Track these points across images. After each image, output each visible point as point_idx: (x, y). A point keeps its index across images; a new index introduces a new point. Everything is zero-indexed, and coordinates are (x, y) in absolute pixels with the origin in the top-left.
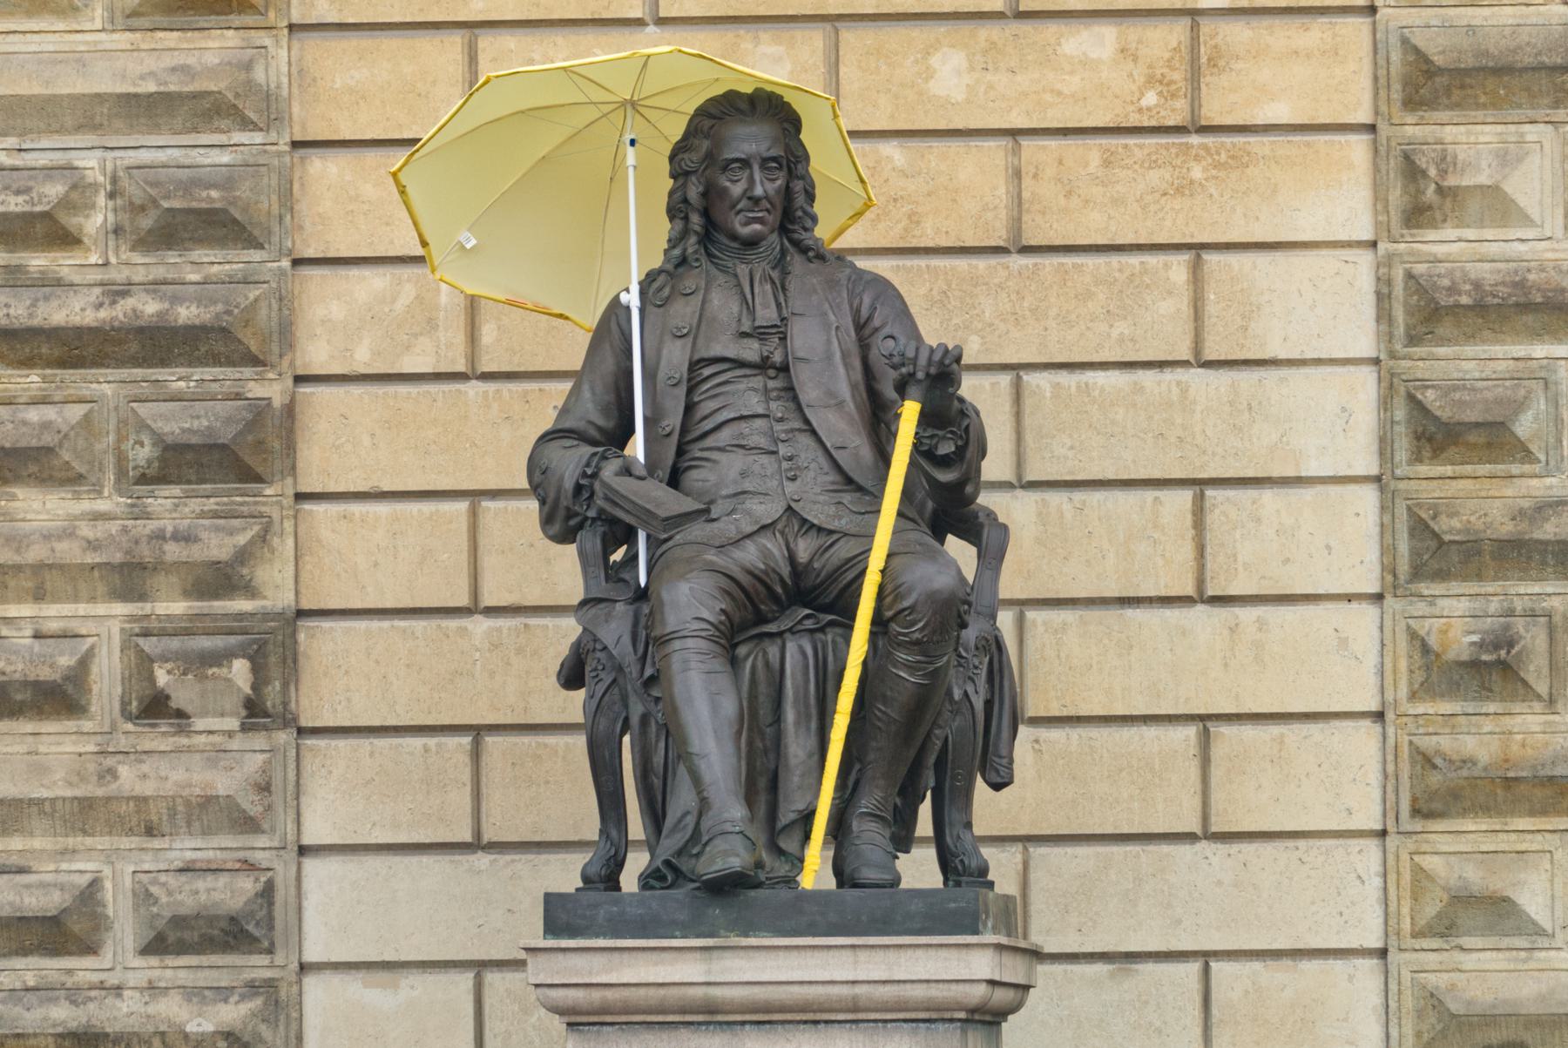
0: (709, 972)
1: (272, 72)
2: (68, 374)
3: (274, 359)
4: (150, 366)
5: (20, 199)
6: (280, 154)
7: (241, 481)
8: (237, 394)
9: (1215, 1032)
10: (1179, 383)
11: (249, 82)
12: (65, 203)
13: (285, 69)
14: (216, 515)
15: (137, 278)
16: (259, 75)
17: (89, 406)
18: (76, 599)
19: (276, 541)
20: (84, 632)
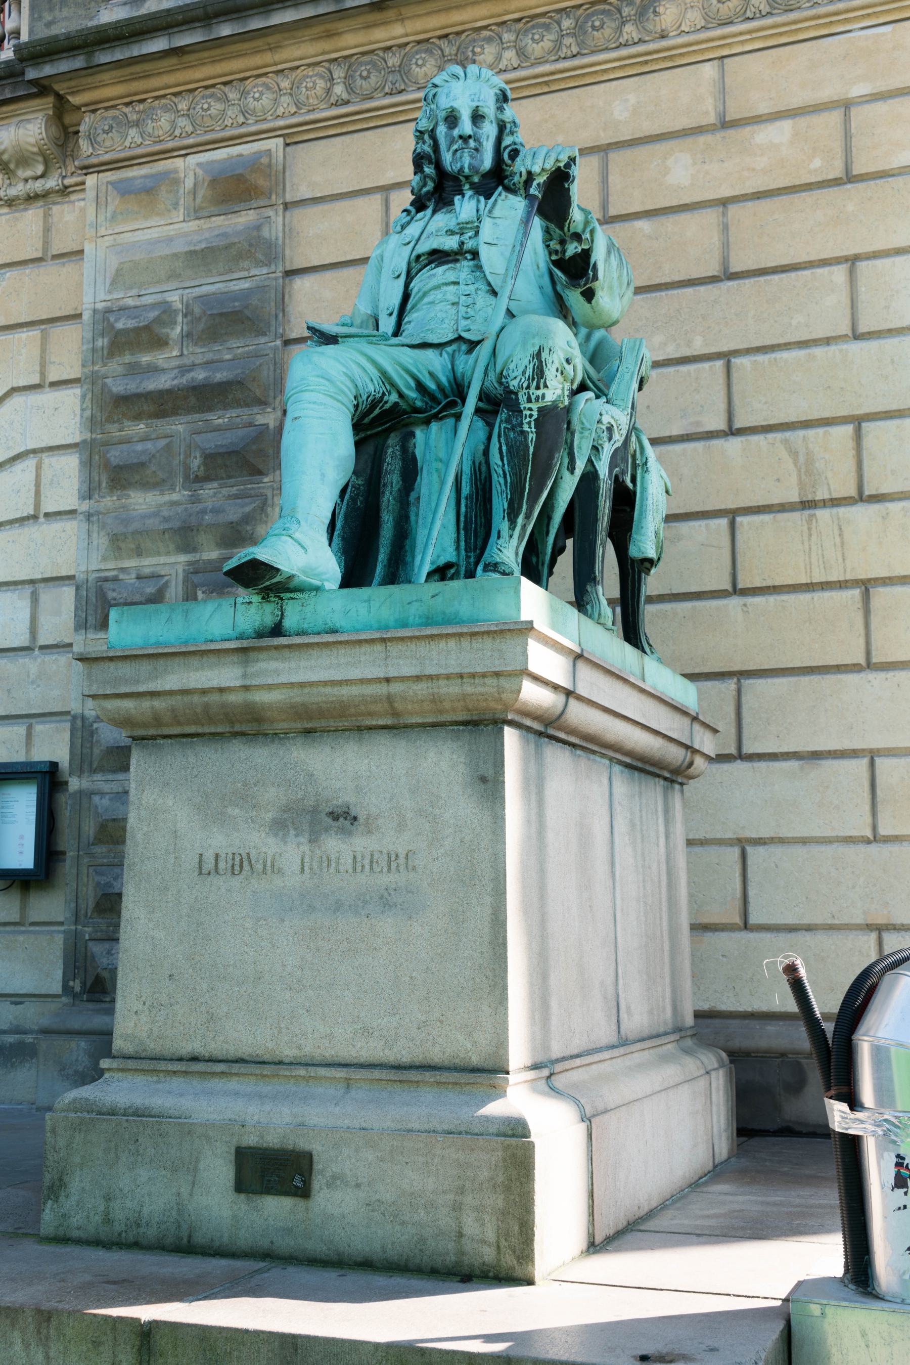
0: (244, 676)
1: (274, 234)
2: (159, 422)
3: (271, 400)
4: (203, 412)
5: (134, 321)
6: (276, 279)
7: (251, 475)
8: (250, 423)
9: (880, 807)
10: (841, 351)
11: (259, 237)
12: (157, 320)
13: (280, 228)
14: (237, 497)
15: (197, 362)
16: (265, 233)
17: (167, 440)
18: (159, 554)
19: (269, 509)
20: (163, 573)
